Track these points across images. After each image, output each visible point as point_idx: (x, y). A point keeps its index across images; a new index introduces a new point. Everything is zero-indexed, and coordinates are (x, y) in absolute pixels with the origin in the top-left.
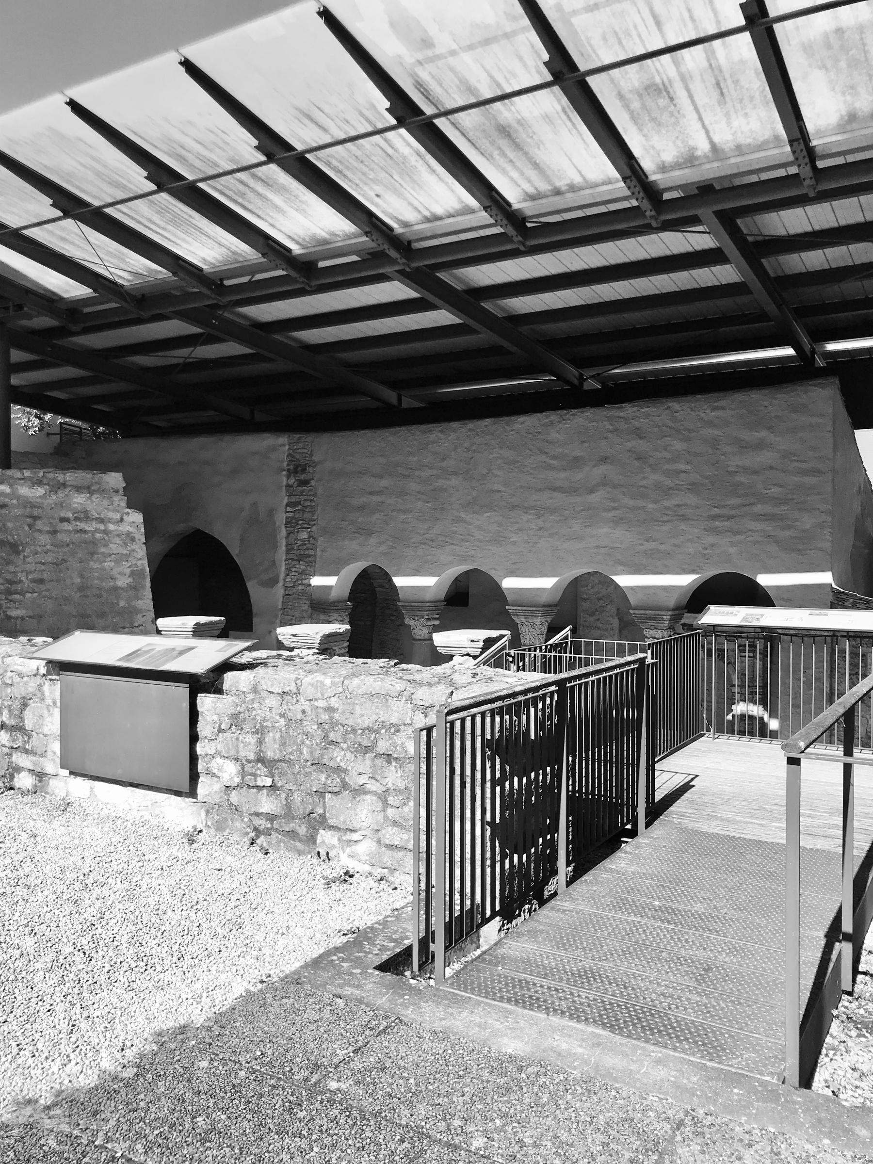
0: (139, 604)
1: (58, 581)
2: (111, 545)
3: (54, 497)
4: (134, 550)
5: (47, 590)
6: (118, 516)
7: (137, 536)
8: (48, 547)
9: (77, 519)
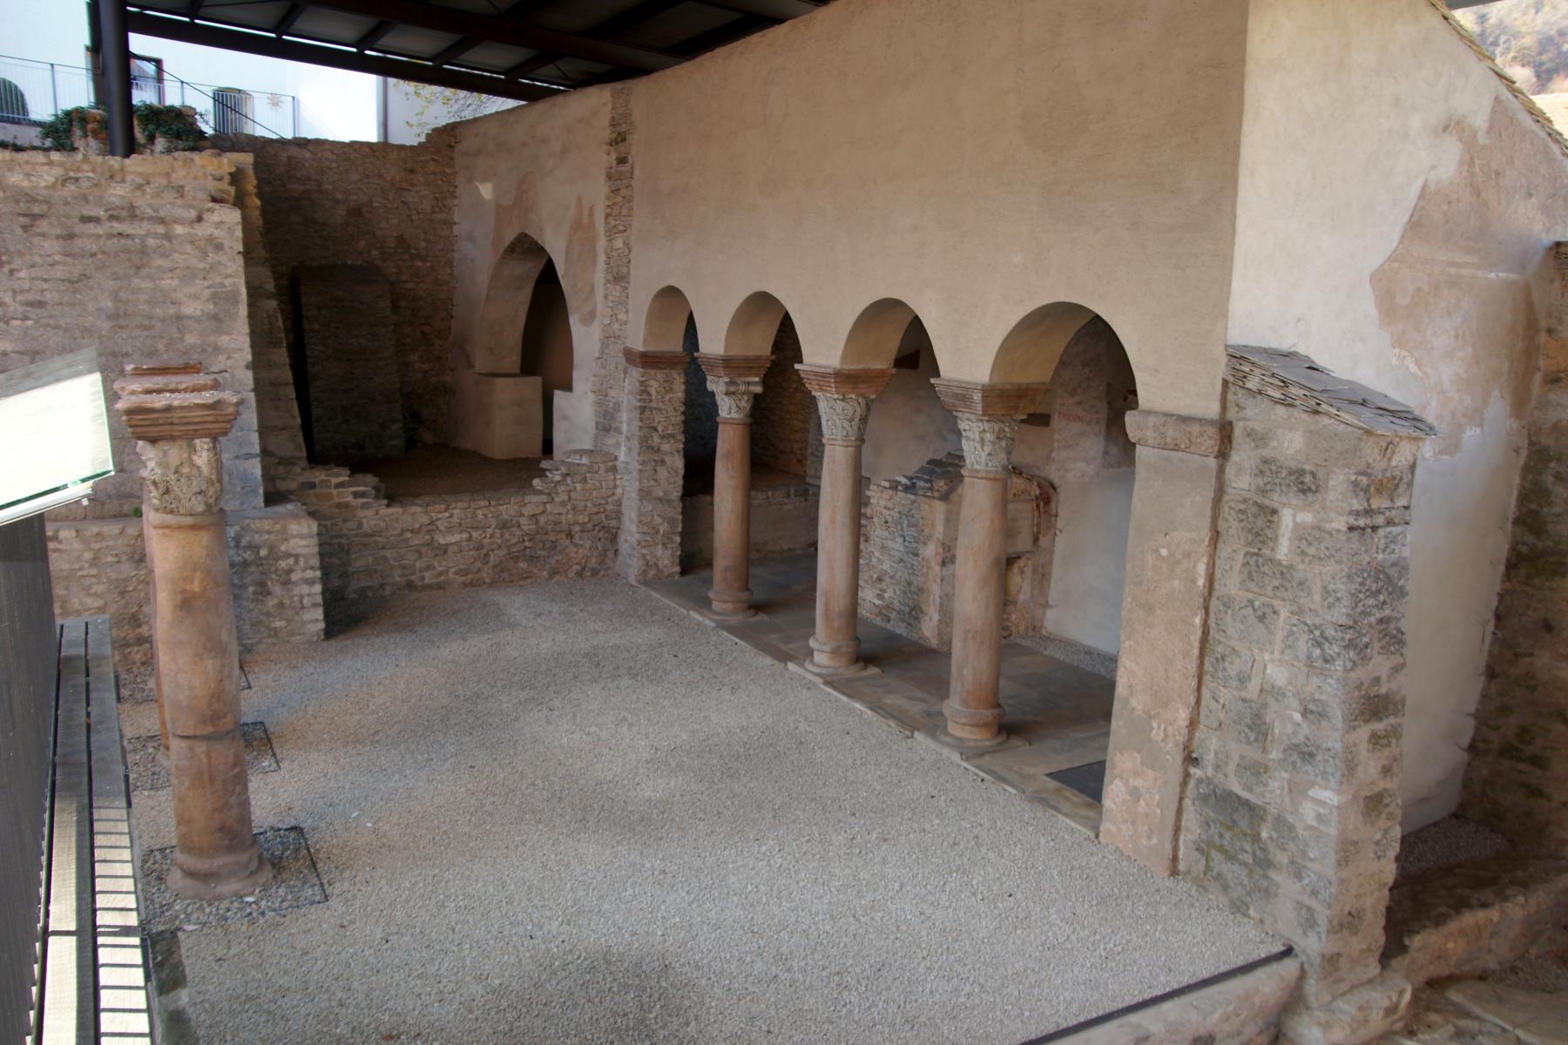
0: (224, 340)
1: (72, 305)
2: (176, 255)
3: (73, 188)
4: (220, 263)
5: (51, 317)
6: (193, 214)
7: (227, 243)
8: (57, 257)
9: (112, 218)
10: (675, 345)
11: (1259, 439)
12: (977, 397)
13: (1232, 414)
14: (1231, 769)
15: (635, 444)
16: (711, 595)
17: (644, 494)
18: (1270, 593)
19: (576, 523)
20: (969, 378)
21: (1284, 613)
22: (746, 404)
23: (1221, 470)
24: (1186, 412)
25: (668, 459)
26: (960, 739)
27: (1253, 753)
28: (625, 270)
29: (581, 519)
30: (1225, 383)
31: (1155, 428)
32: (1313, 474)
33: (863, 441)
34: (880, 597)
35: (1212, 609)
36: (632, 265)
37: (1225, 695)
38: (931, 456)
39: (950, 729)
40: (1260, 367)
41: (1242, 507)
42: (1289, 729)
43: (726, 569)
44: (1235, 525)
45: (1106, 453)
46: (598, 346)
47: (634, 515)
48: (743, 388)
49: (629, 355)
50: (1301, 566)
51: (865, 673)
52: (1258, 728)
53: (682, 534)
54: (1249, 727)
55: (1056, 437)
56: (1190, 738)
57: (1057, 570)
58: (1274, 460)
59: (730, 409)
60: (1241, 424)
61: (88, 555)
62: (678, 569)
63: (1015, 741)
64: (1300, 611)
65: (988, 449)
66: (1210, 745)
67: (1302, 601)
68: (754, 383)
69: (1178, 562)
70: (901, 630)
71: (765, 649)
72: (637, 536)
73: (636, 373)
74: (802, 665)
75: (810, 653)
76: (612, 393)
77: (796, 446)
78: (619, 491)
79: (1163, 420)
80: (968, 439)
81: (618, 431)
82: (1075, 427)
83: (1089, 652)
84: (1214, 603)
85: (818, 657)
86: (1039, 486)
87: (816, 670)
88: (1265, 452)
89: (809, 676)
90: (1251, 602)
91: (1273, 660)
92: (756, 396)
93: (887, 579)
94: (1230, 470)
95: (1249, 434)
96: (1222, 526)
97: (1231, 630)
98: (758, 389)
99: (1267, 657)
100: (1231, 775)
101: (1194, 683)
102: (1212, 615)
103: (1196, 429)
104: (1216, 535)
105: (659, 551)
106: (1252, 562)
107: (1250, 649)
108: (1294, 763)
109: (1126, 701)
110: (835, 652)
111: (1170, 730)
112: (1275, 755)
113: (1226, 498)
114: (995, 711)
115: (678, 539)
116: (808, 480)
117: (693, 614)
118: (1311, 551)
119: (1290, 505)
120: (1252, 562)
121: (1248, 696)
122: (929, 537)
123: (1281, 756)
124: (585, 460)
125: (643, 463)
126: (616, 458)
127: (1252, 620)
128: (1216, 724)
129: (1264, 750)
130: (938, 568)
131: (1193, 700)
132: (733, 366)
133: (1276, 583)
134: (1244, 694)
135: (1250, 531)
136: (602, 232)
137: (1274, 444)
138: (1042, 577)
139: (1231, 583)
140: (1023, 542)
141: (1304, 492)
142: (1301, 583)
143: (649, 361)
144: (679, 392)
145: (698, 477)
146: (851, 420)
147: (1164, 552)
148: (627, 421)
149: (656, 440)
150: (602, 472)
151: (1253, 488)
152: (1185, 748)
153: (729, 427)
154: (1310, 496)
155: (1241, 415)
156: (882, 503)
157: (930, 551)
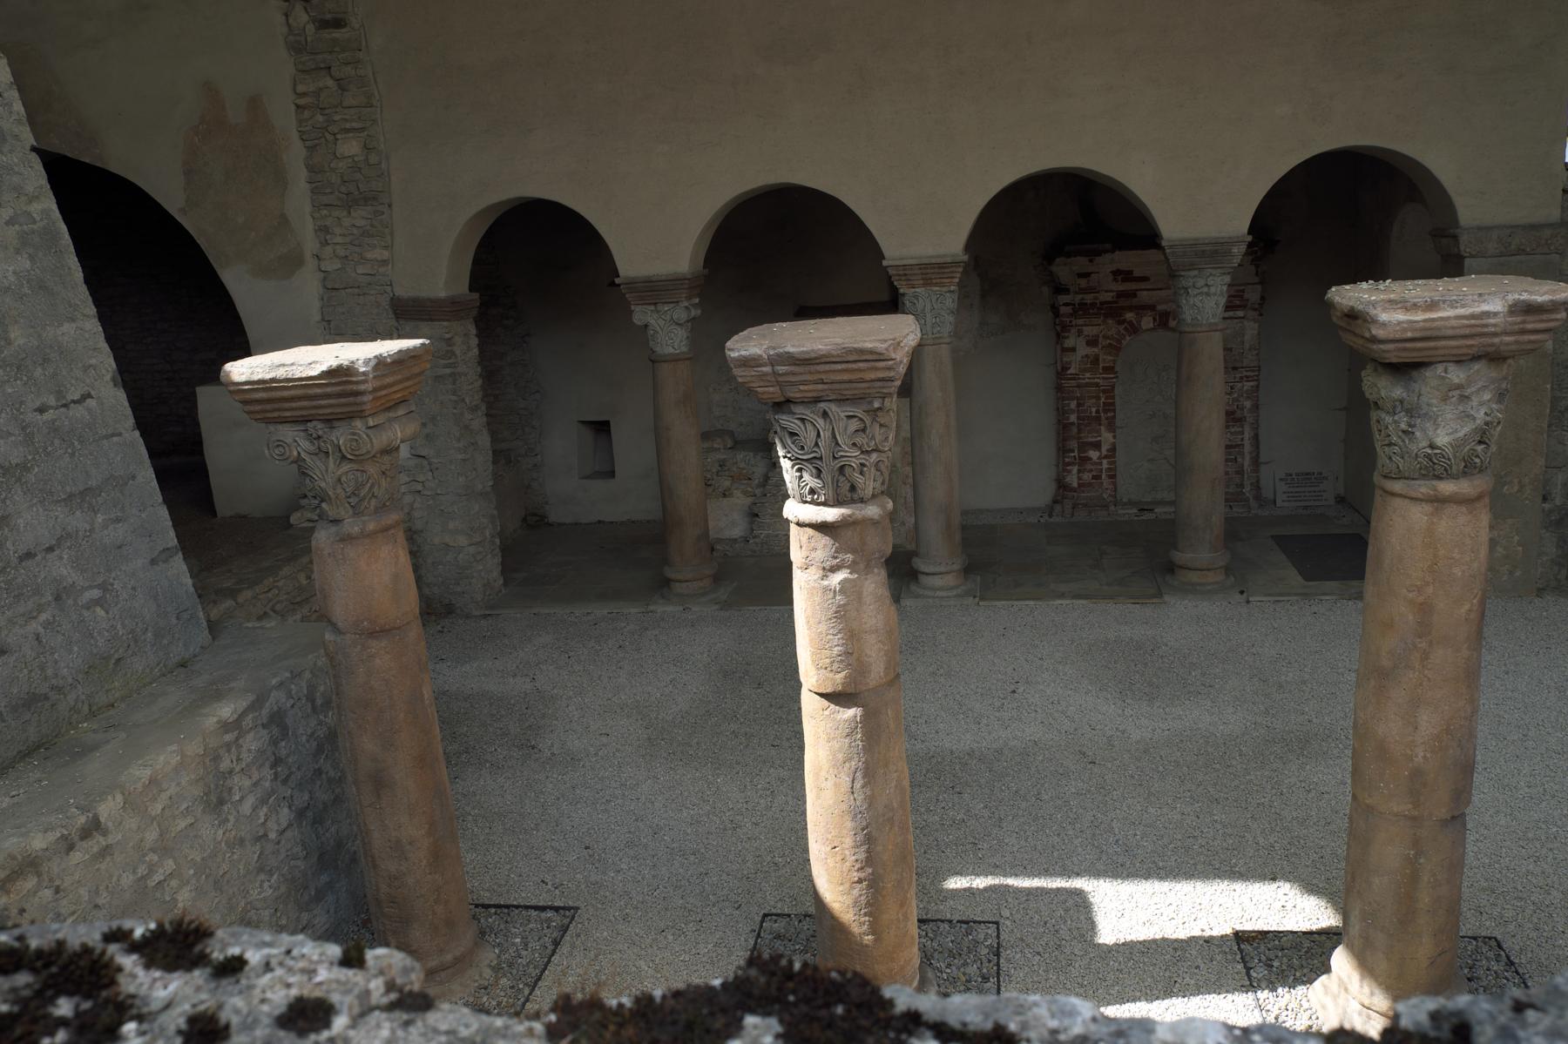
61: (151, 835)
115: (498, 541)
136: (295, 135)
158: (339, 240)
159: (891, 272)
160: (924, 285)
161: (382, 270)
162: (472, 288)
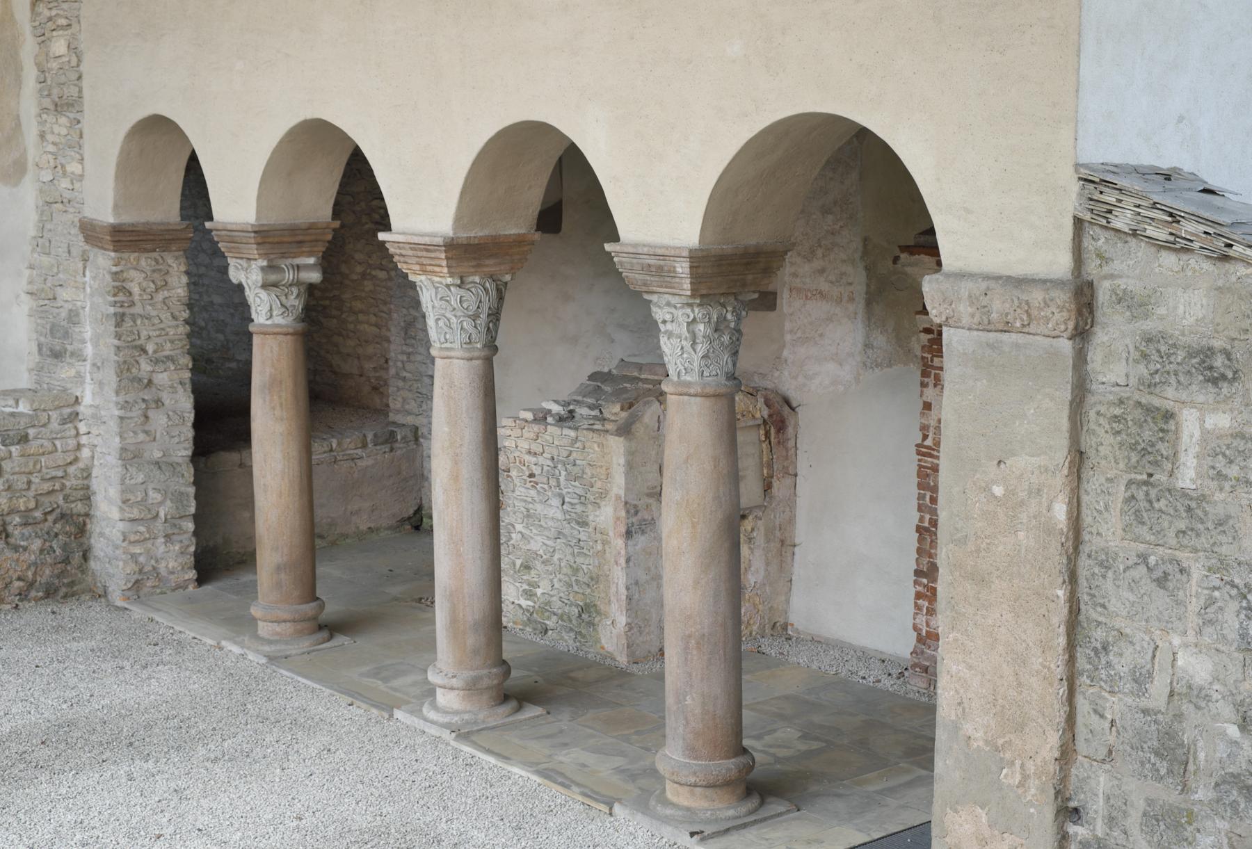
10: (166, 209)
11: (1136, 305)
12: (682, 268)
13: (1092, 269)
14: (1133, 821)
15: (110, 376)
16: (255, 611)
17: (130, 457)
18: (1173, 542)
19: (12, 512)
20: (667, 241)
21: (1197, 572)
22: (295, 301)
23: (1080, 358)
24: (1018, 270)
25: (166, 397)
26: (688, 809)
27: (1168, 795)
28: (74, 91)
29: (21, 504)
30: (1078, 223)
31: (972, 299)
32: (1228, 354)
33: (496, 349)
34: (529, 594)
35: (1083, 573)
36: (85, 83)
37: (1115, 706)
38: (591, 369)
39: (669, 795)
40: (1131, 194)
41: (1118, 411)
42: (1222, 751)
43: (279, 568)
44: (1109, 439)
45: (868, 346)
46: (34, 217)
47: (114, 492)
48: (289, 276)
49: (90, 231)
50: (1219, 496)
51: (521, 716)
52: (1172, 754)
53: (197, 518)
54: (1157, 754)
55: (788, 326)
56: (1064, 779)
57: (802, 532)
58: (1163, 336)
59: (271, 312)
60: (1107, 284)
62: (192, 574)
63: (776, 806)
64: (1223, 565)
65: (701, 349)
66: (1097, 787)
67: (1224, 550)
68: (308, 267)
69: (1022, 503)
70: (567, 643)
71: (355, 694)
72: (121, 526)
73: (104, 260)
74: (417, 712)
75: (430, 692)
76: (64, 294)
77: (368, 366)
78: (86, 453)
79: (984, 285)
80: (670, 335)
81: (79, 356)
82: (817, 309)
83: (864, 655)
84: (1084, 563)
85: (443, 698)
86: (768, 403)
87: (446, 719)
88: (1149, 325)
89: (433, 731)
90: (1143, 558)
91: (1186, 646)
92: (311, 288)
93: (538, 564)
94: (1095, 357)
95: (1121, 298)
96: (1087, 442)
97: (1118, 603)
98: (315, 277)
99: (1177, 641)
100: (1135, 831)
101: (1063, 690)
102: (1083, 583)
103: (1037, 296)
104: (1079, 458)
105: (160, 547)
106: (1140, 495)
107: (1147, 631)
108: (1234, 805)
109: (956, 727)
110: (471, 688)
111: (1031, 768)
112: (1203, 793)
113: (1091, 399)
114: (742, 760)
115: (190, 526)
116: (392, 417)
117: (228, 646)
118: (1233, 471)
119: (1193, 405)
120: (1140, 495)
121: (1151, 704)
122: (603, 495)
123: (1211, 795)
124: (23, 408)
125: (125, 406)
126: (77, 401)
127: (1147, 585)
128: (1103, 752)
129: (1185, 789)
130: (620, 543)
131: (1060, 715)
132: (274, 241)
133: (1182, 525)
134: (1144, 703)
135: (1133, 447)
137: (1162, 311)
138: (784, 546)
139: (1109, 530)
140: (750, 491)
141: (1214, 381)
142: (1220, 524)
143: (125, 239)
144: (179, 286)
145: (220, 422)
146: (475, 317)
147: (998, 490)
148: (94, 339)
149: (146, 367)
150: (55, 425)
151: (1133, 381)
152: (1058, 793)
153: (270, 340)
154: (1225, 386)
155: (1106, 270)
156: (524, 445)
157: (607, 516)
158: (51, 148)
159: (392, 250)
160: (425, 272)
161: (77, 185)
162: (183, 218)
